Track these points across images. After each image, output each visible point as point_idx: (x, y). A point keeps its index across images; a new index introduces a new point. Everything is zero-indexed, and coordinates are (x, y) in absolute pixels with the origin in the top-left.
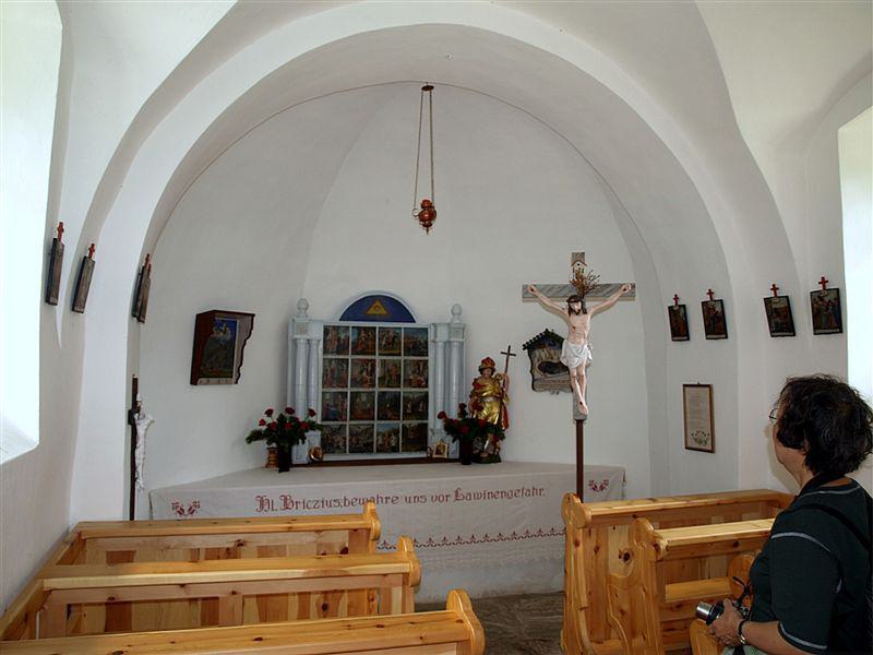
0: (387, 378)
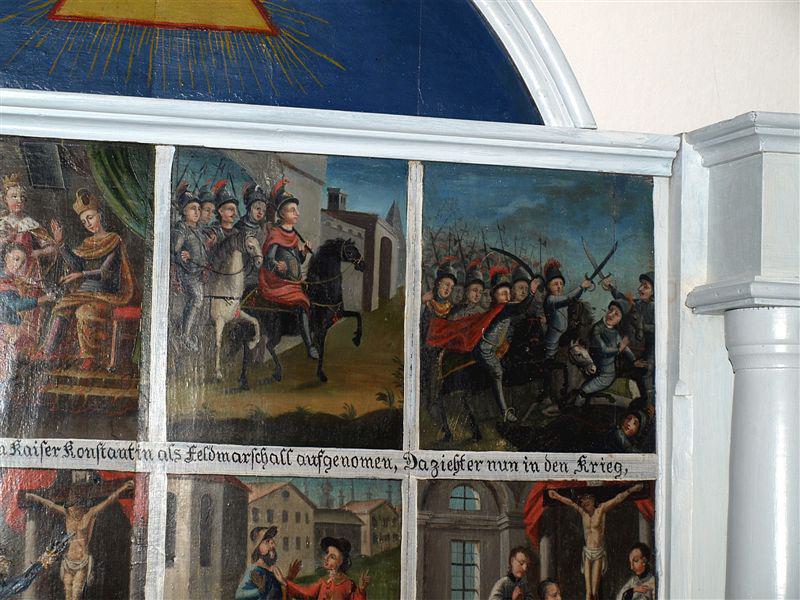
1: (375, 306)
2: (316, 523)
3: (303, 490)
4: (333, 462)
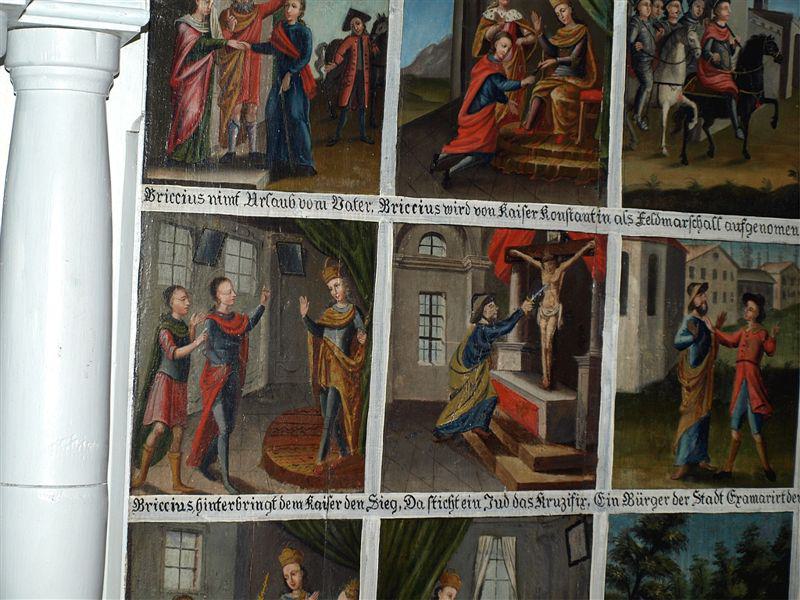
0: (692, 409)
1: (789, 95)
2: (739, 281)
3: (729, 253)
4: (753, 228)
